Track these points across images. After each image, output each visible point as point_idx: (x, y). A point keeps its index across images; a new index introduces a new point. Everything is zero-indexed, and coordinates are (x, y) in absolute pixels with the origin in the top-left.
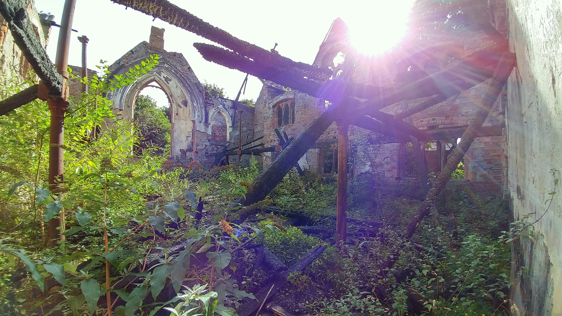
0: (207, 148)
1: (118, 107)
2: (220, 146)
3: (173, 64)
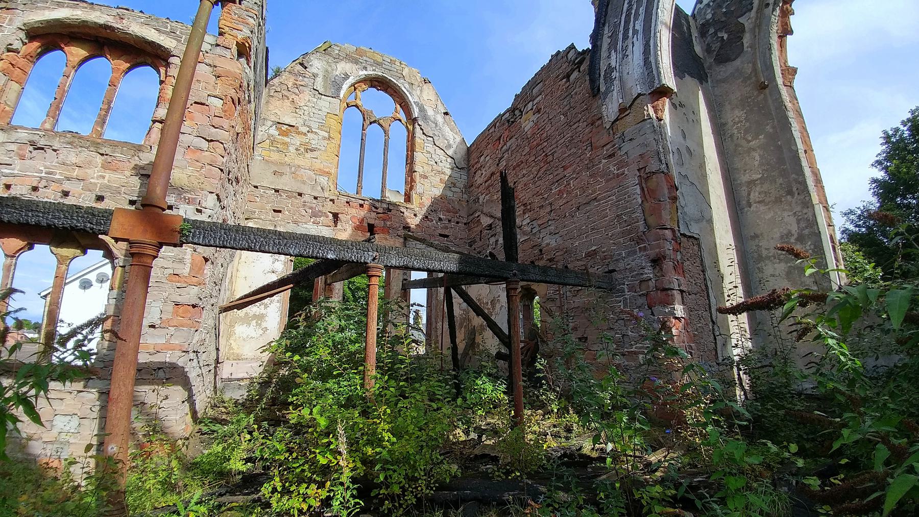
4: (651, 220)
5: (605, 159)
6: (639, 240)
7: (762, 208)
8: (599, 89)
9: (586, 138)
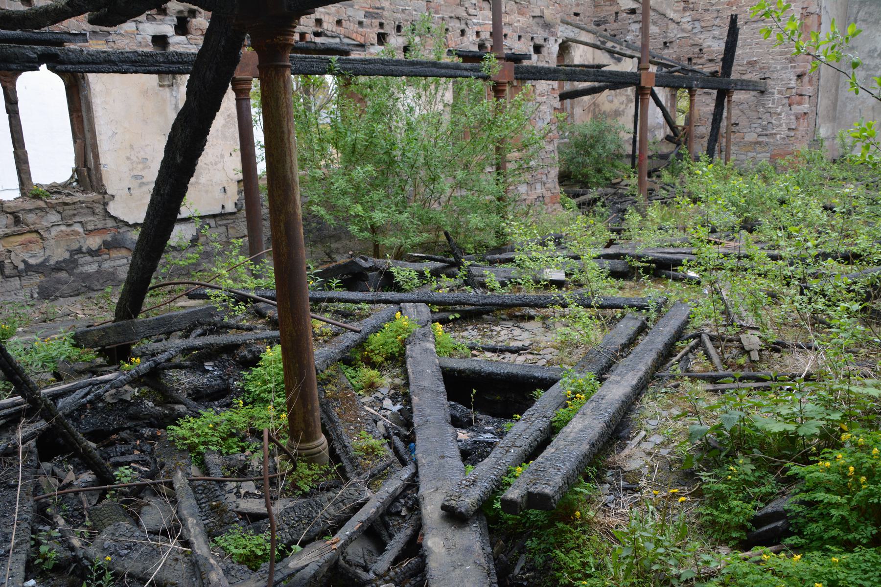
6: (792, 60)
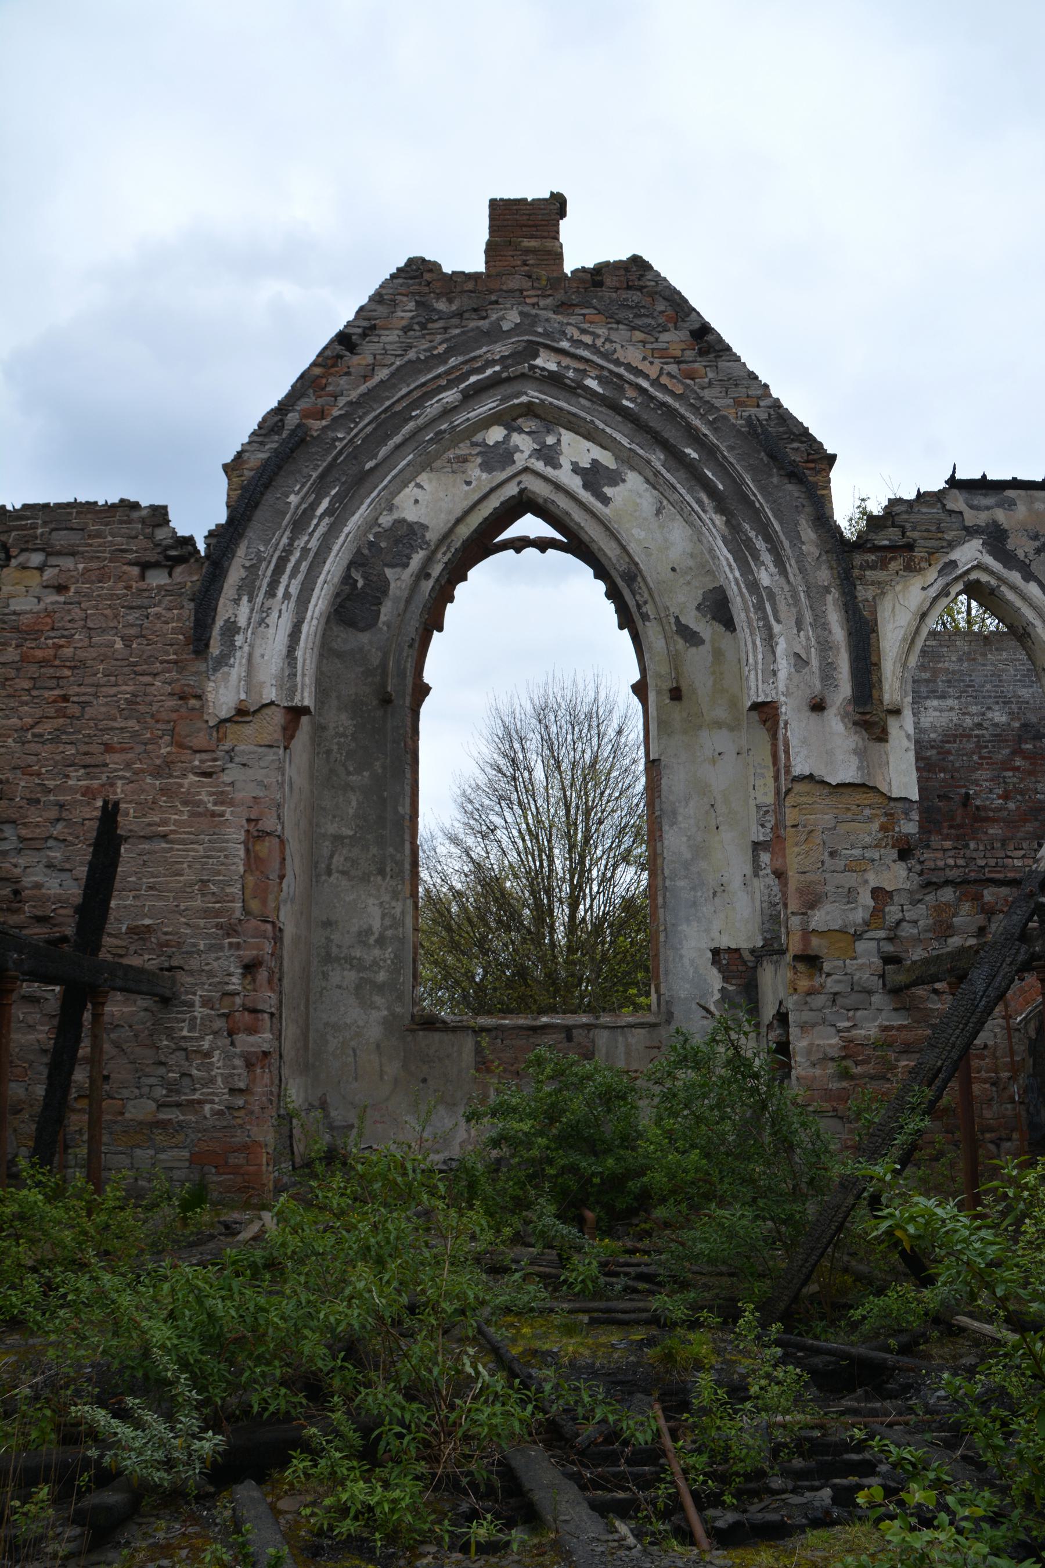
0: (893, 912)
1: (271, 694)
2: (1004, 891)
3: (588, 339)
4: (254, 905)
5: (196, 774)
6: (231, 930)
7: (345, 883)
8: (207, 645)
9: (164, 716)
